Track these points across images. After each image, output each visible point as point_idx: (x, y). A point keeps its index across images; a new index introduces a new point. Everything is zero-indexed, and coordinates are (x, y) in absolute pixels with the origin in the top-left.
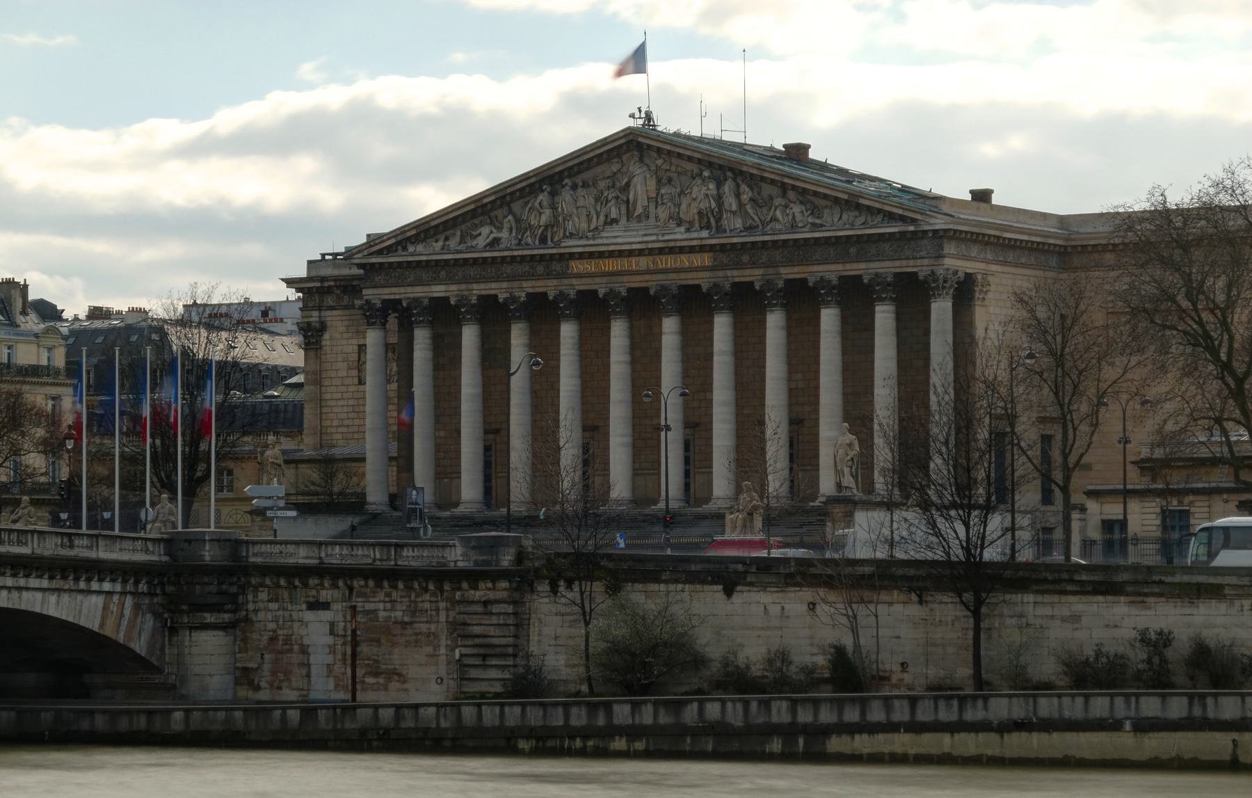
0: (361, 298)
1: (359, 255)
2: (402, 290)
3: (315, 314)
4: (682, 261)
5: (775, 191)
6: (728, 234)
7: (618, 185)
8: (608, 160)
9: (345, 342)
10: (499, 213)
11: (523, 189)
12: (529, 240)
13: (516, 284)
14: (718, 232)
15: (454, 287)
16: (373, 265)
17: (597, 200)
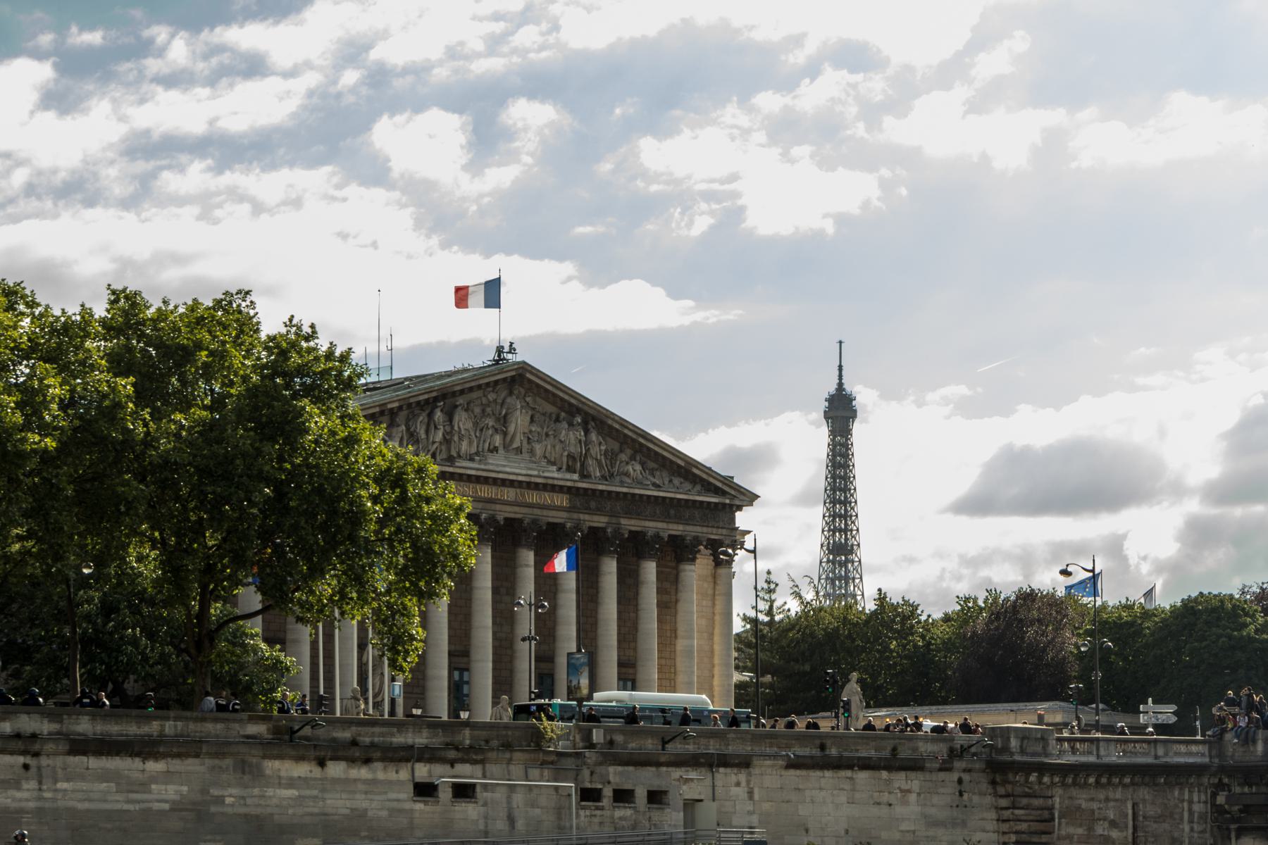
5: (616, 446)
11: (418, 403)
17: (476, 424)
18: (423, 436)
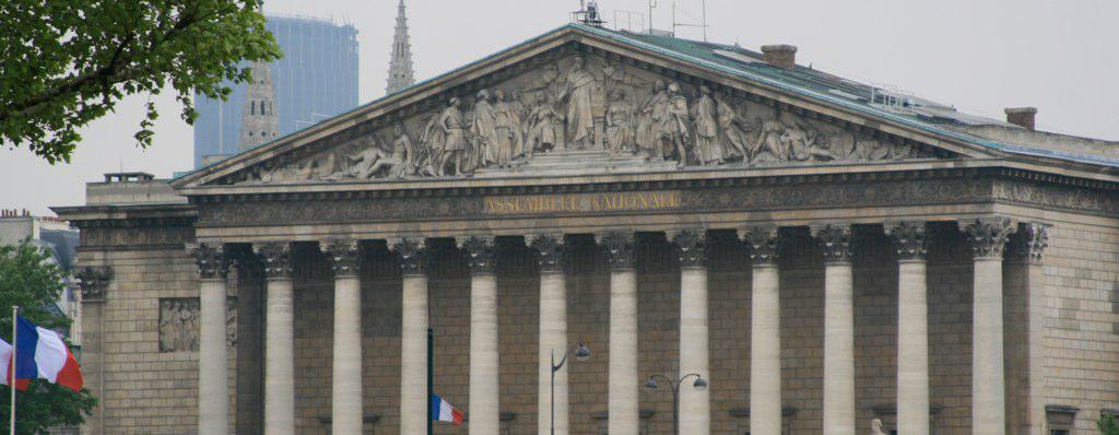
0: (192, 238)
1: (194, 185)
2: (252, 231)
3: (98, 255)
4: (638, 201)
5: (765, 112)
6: (702, 167)
7: (551, 97)
8: (538, 67)
9: (139, 294)
10: (387, 132)
12: (430, 169)
13: (411, 226)
14: (688, 163)
15: (325, 229)
16: (213, 196)
17: (523, 118)
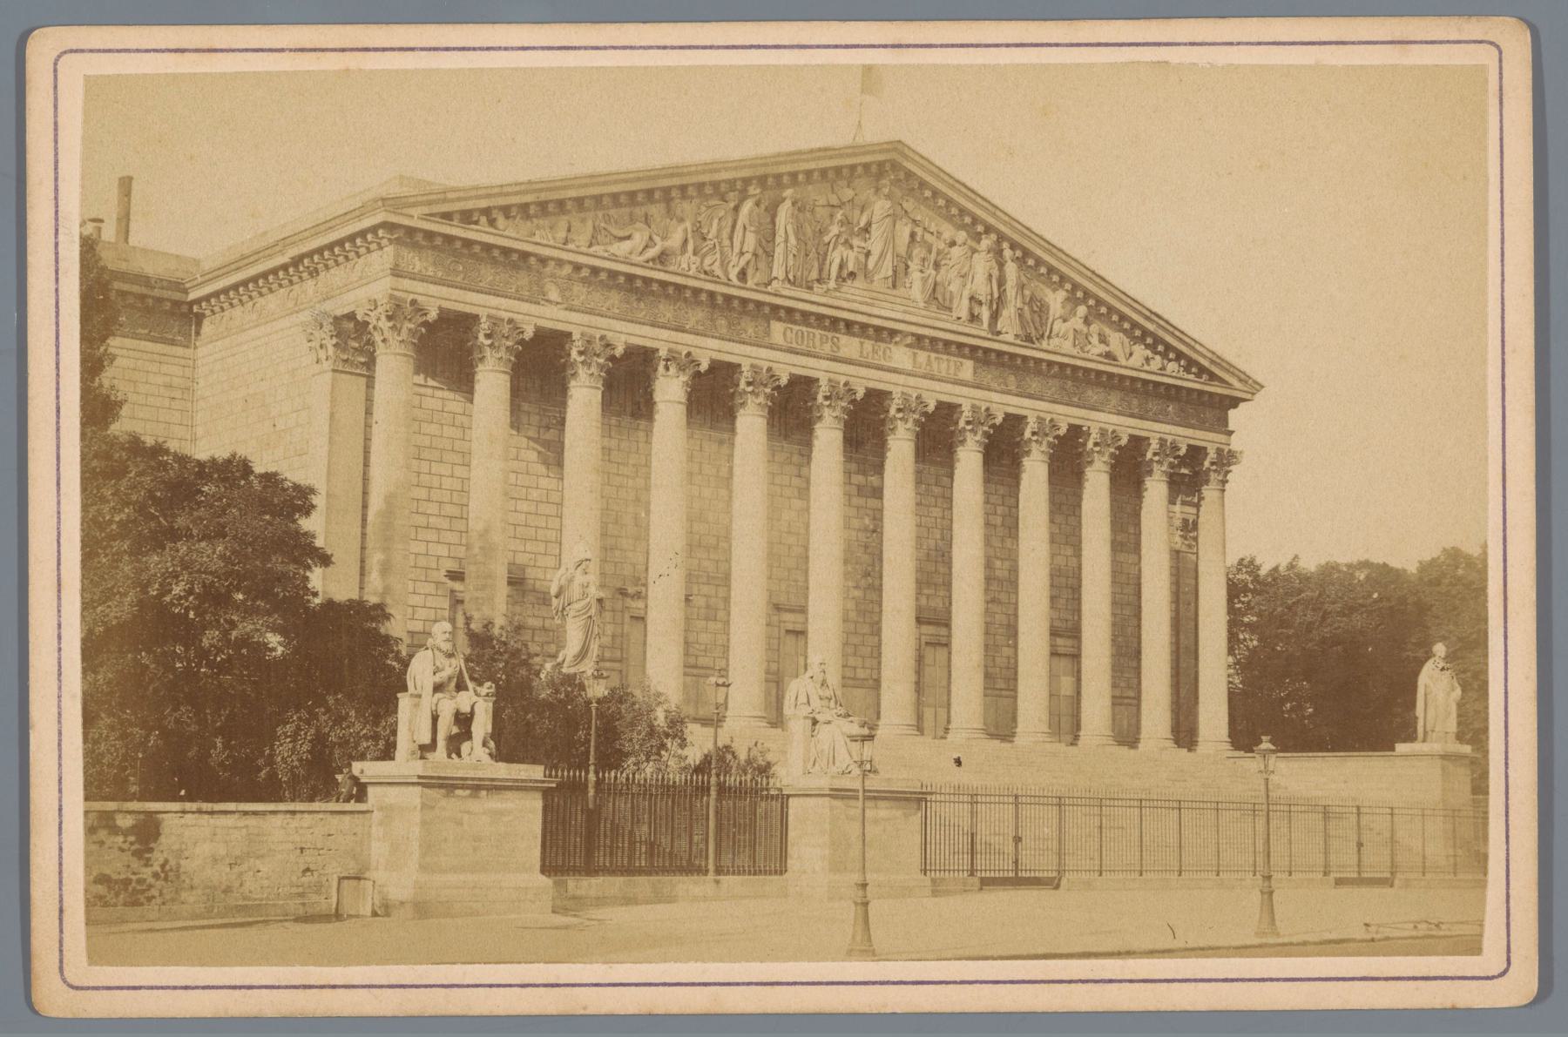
10: (656, 210)
18: (726, 242)
